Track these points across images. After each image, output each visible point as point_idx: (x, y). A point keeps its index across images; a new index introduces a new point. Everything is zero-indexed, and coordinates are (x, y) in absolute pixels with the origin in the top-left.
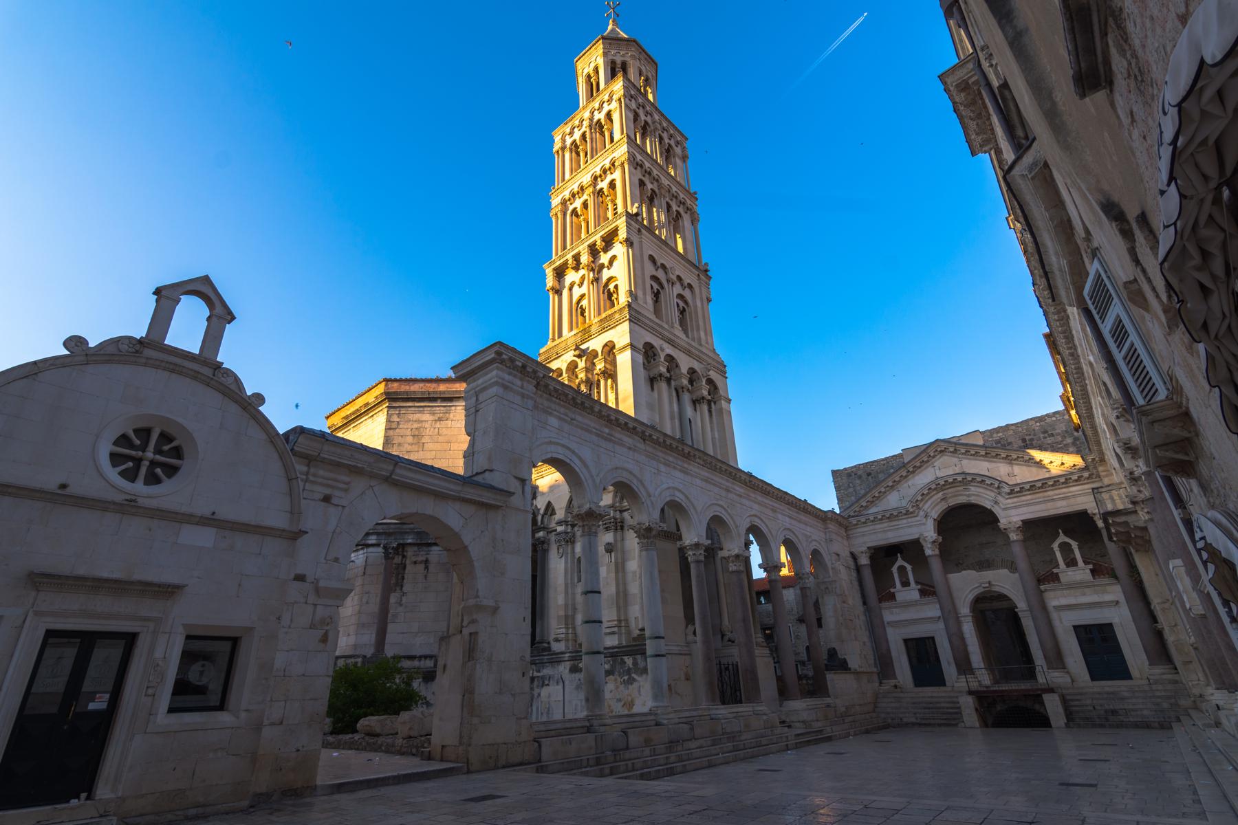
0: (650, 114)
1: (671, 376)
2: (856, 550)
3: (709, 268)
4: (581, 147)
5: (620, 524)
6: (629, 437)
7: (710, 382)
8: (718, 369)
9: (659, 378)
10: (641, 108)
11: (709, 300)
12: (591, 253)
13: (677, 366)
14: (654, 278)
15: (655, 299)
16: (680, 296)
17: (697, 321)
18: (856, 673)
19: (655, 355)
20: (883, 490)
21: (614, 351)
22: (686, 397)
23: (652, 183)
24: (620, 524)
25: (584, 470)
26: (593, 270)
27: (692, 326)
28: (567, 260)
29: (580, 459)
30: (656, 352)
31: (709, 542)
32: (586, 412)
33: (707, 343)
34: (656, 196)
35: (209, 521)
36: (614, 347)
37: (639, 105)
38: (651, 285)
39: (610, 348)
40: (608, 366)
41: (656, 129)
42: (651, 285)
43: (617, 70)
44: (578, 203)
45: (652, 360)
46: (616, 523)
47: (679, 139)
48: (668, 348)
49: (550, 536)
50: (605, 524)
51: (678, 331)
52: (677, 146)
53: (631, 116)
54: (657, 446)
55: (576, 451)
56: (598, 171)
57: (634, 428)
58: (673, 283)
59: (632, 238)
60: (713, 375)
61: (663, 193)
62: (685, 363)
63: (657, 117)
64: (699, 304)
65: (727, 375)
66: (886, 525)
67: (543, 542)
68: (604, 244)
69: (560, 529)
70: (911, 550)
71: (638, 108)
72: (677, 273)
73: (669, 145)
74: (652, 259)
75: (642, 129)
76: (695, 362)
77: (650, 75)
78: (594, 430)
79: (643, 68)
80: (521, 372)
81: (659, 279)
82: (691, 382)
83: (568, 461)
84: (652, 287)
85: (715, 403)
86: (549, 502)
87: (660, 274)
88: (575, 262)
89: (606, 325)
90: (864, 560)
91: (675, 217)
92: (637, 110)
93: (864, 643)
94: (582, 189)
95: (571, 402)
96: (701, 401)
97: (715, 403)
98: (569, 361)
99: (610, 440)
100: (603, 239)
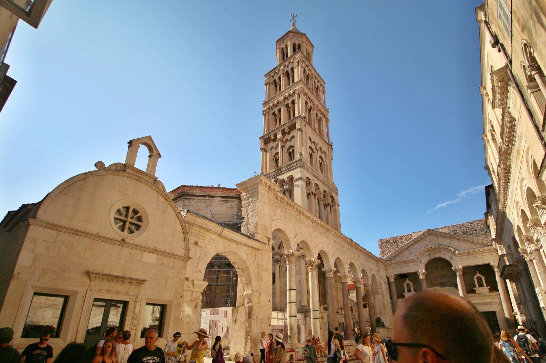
2: (389, 276)
4: (278, 83)
7: (332, 197)
8: (335, 191)
9: (312, 194)
10: (307, 67)
11: (332, 159)
12: (282, 134)
14: (311, 148)
16: (320, 157)
17: (327, 169)
18: (388, 328)
19: (310, 183)
20: (403, 250)
22: (322, 203)
23: (311, 103)
26: (282, 141)
30: (311, 182)
31: (336, 269)
33: (331, 179)
35: (154, 251)
39: (291, 178)
40: (289, 186)
41: (312, 77)
43: (296, 47)
47: (322, 83)
53: (303, 70)
62: (322, 188)
63: (313, 72)
66: (403, 265)
70: (414, 276)
73: (318, 86)
79: (308, 48)
82: (324, 196)
85: (333, 207)
87: (313, 146)
89: (290, 168)
90: (392, 280)
93: (390, 316)
94: (278, 103)
97: (333, 207)
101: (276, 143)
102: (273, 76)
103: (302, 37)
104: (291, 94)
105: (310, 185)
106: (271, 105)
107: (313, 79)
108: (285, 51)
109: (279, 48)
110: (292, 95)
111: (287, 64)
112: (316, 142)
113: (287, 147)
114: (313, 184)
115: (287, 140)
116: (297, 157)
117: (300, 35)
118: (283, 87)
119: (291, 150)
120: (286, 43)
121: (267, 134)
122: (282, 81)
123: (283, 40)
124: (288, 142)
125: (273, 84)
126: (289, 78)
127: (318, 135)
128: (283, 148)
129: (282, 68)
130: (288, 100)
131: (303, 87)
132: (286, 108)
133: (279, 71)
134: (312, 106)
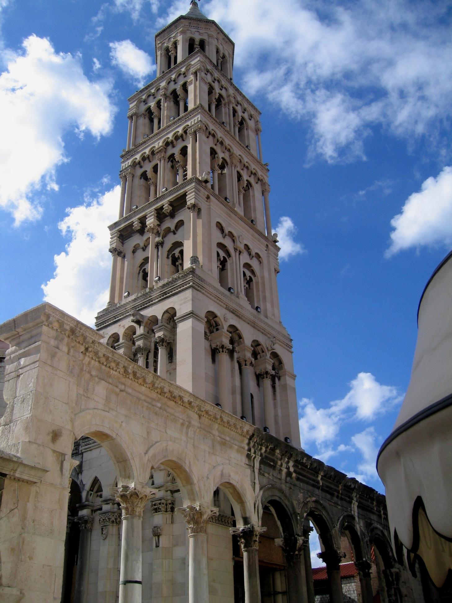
1: (233, 348)
3: (278, 239)
4: (154, 115)
5: (170, 506)
7: (275, 355)
9: (221, 350)
10: (216, 82)
12: (157, 217)
13: (240, 337)
14: (221, 246)
15: (221, 266)
17: (264, 292)
19: (217, 324)
21: (175, 318)
23: (223, 152)
24: (170, 506)
27: (258, 296)
28: (133, 222)
33: (274, 315)
34: (227, 165)
36: (175, 314)
37: (215, 79)
39: (171, 315)
41: (230, 102)
43: (195, 46)
44: (148, 167)
45: (215, 330)
46: (166, 505)
48: (232, 319)
49: (94, 515)
50: (155, 505)
51: (243, 301)
52: (250, 120)
53: (206, 88)
56: (170, 136)
57: (190, 403)
58: (240, 252)
59: (200, 204)
60: (279, 349)
61: (234, 162)
63: (231, 91)
64: (266, 274)
65: (293, 350)
67: (86, 522)
68: (171, 208)
69: (106, 508)
71: (214, 82)
72: (246, 242)
74: (220, 227)
75: (216, 101)
76: (260, 334)
80: (69, 336)
81: (226, 247)
82: (255, 355)
84: (218, 255)
85: (279, 379)
86: (96, 477)
88: (140, 225)
91: (245, 186)
92: (213, 84)
94: (153, 153)
95: (122, 370)
96: (265, 375)
97: (279, 379)
98: (127, 327)
100: (171, 204)
101: (145, 237)
102: (145, 102)
103: (207, 27)
104: (179, 134)
105: (217, 330)
106: (138, 157)
108: (172, 53)
109: (161, 47)
110: (182, 136)
111: (173, 77)
112: (235, 234)
113: (168, 245)
114: (226, 327)
115: (168, 231)
116: (187, 264)
117: (205, 23)
118: (165, 121)
119: (177, 252)
120: (175, 37)
121: (127, 219)
122: (164, 110)
123: (171, 31)
124: (171, 235)
125: (145, 115)
126: (177, 103)
127: (241, 218)
128: (160, 248)
129: (163, 84)
130: (173, 147)
131: (204, 120)
132: (170, 162)
133: (158, 90)
134: (228, 160)
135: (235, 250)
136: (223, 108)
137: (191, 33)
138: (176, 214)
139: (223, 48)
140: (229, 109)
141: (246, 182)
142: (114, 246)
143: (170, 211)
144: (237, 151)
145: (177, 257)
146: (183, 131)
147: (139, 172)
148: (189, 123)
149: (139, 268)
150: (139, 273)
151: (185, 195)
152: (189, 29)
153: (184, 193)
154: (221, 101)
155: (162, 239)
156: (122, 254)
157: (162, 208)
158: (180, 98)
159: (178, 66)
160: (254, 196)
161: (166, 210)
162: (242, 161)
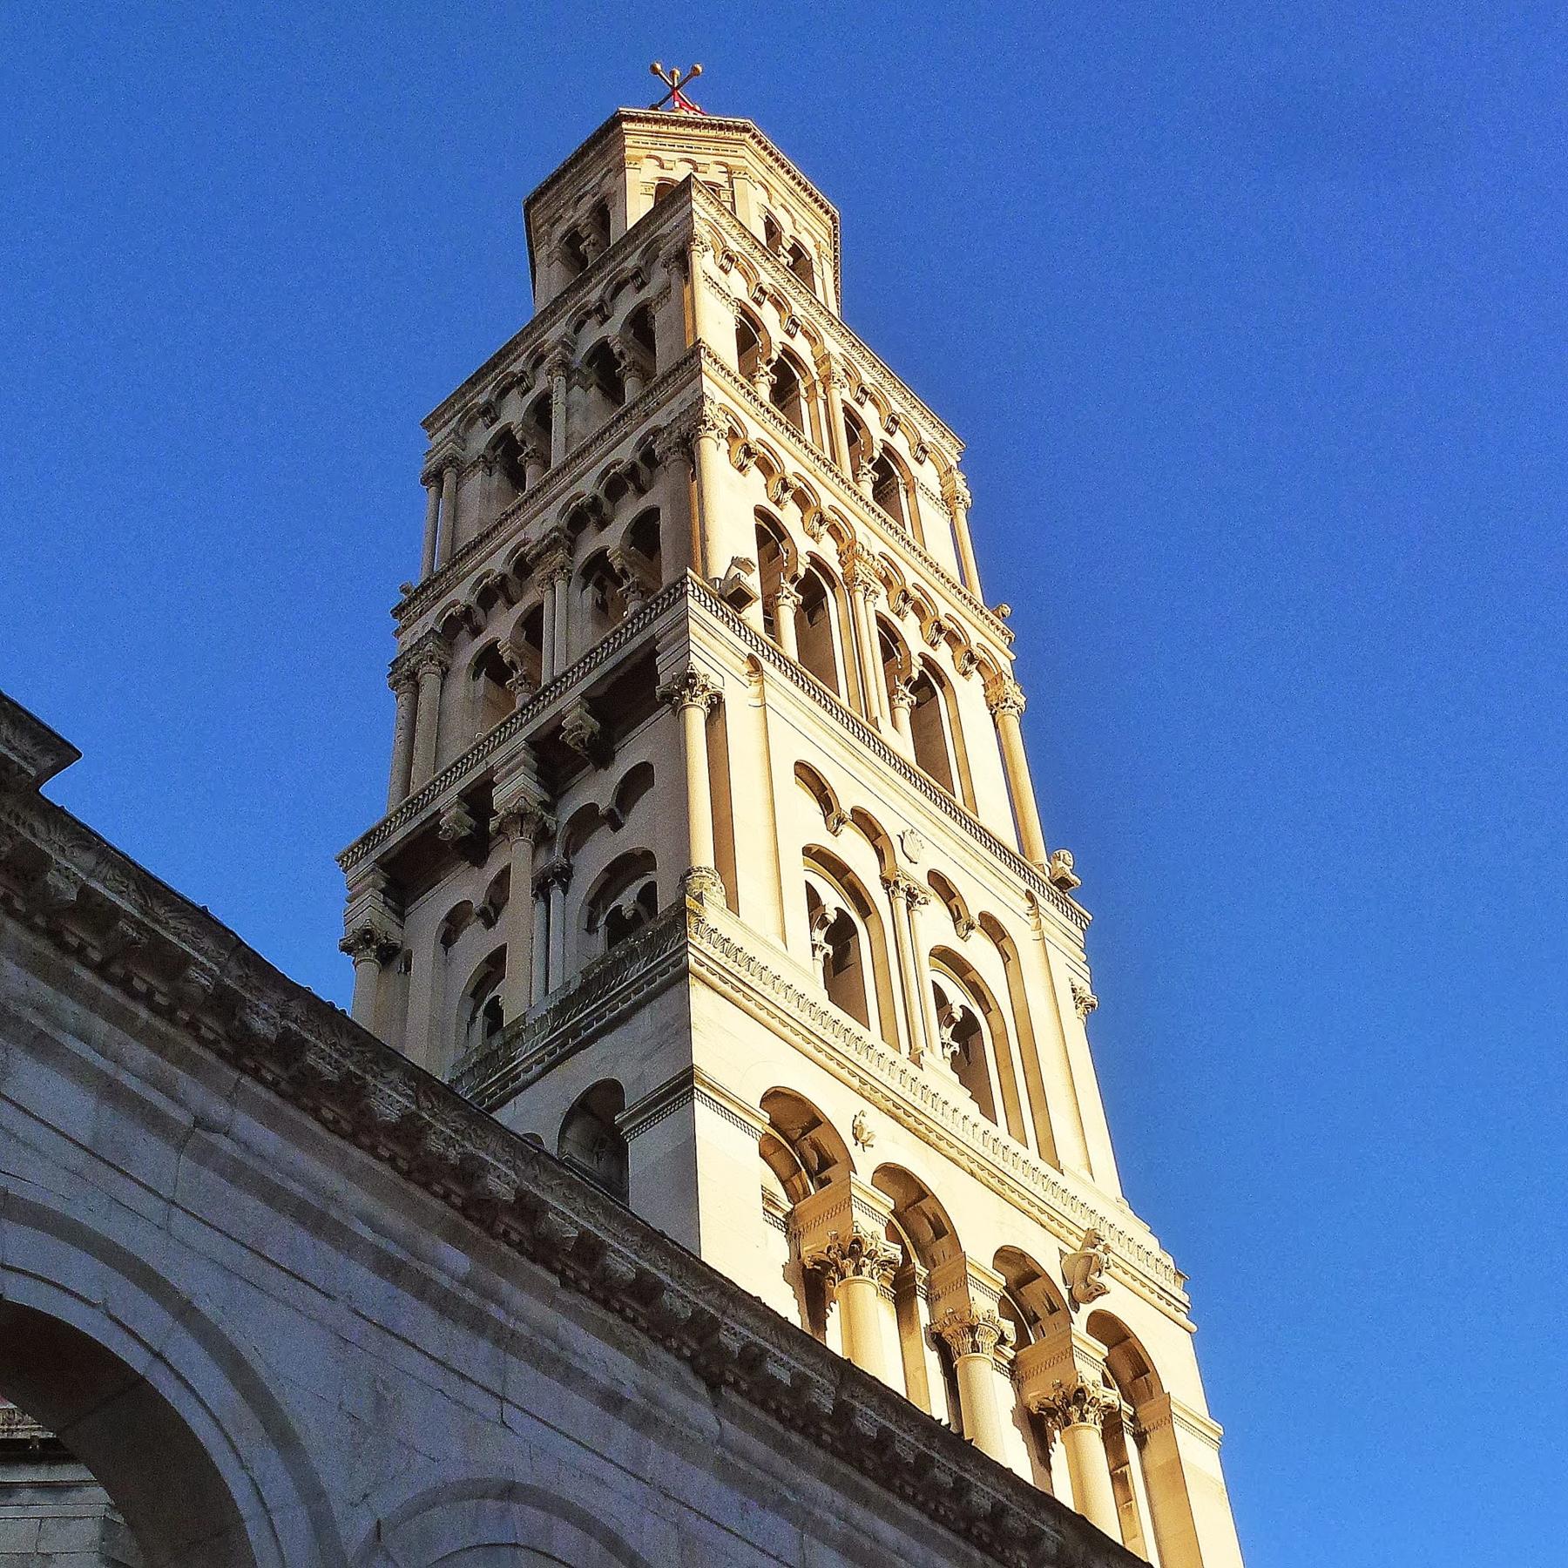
0: (806, 334)
6: (607, 1335)
10: (767, 305)
19: (826, 1163)
23: (813, 537)
25: (252, 1439)
26: (543, 838)
28: (437, 814)
29: (235, 1365)
30: (830, 1148)
32: (315, 1113)
38: (809, 887)
42: (809, 887)
44: (502, 627)
52: (921, 463)
54: (796, 1438)
55: (207, 1308)
58: (911, 895)
68: (593, 724)
71: (759, 304)
74: (807, 774)
77: (808, 243)
78: (366, 1233)
83: (136, 1359)
88: (470, 820)
94: (523, 568)
99: (478, 1323)
100: (594, 703)
101: (492, 870)
102: (490, 412)
107: (841, 395)
111: (594, 296)
115: (587, 821)
119: (627, 900)
128: (556, 894)
129: (558, 330)
130: (603, 524)
135: (887, 889)
136: (802, 400)
137: (662, 167)
138: (616, 747)
139: (794, 222)
140: (826, 404)
141: (917, 663)
142: (361, 921)
143: (593, 734)
144: (871, 534)
145: (628, 915)
146: (638, 455)
147: (469, 650)
148: (659, 419)
149: (471, 1003)
150: (473, 1019)
151: (648, 656)
152: (653, 153)
153: (647, 649)
154: (795, 377)
155: (566, 855)
156: (398, 963)
157: (555, 728)
158: (623, 366)
159: (613, 257)
160: (957, 720)
161: (572, 731)
162: (894, 577)
